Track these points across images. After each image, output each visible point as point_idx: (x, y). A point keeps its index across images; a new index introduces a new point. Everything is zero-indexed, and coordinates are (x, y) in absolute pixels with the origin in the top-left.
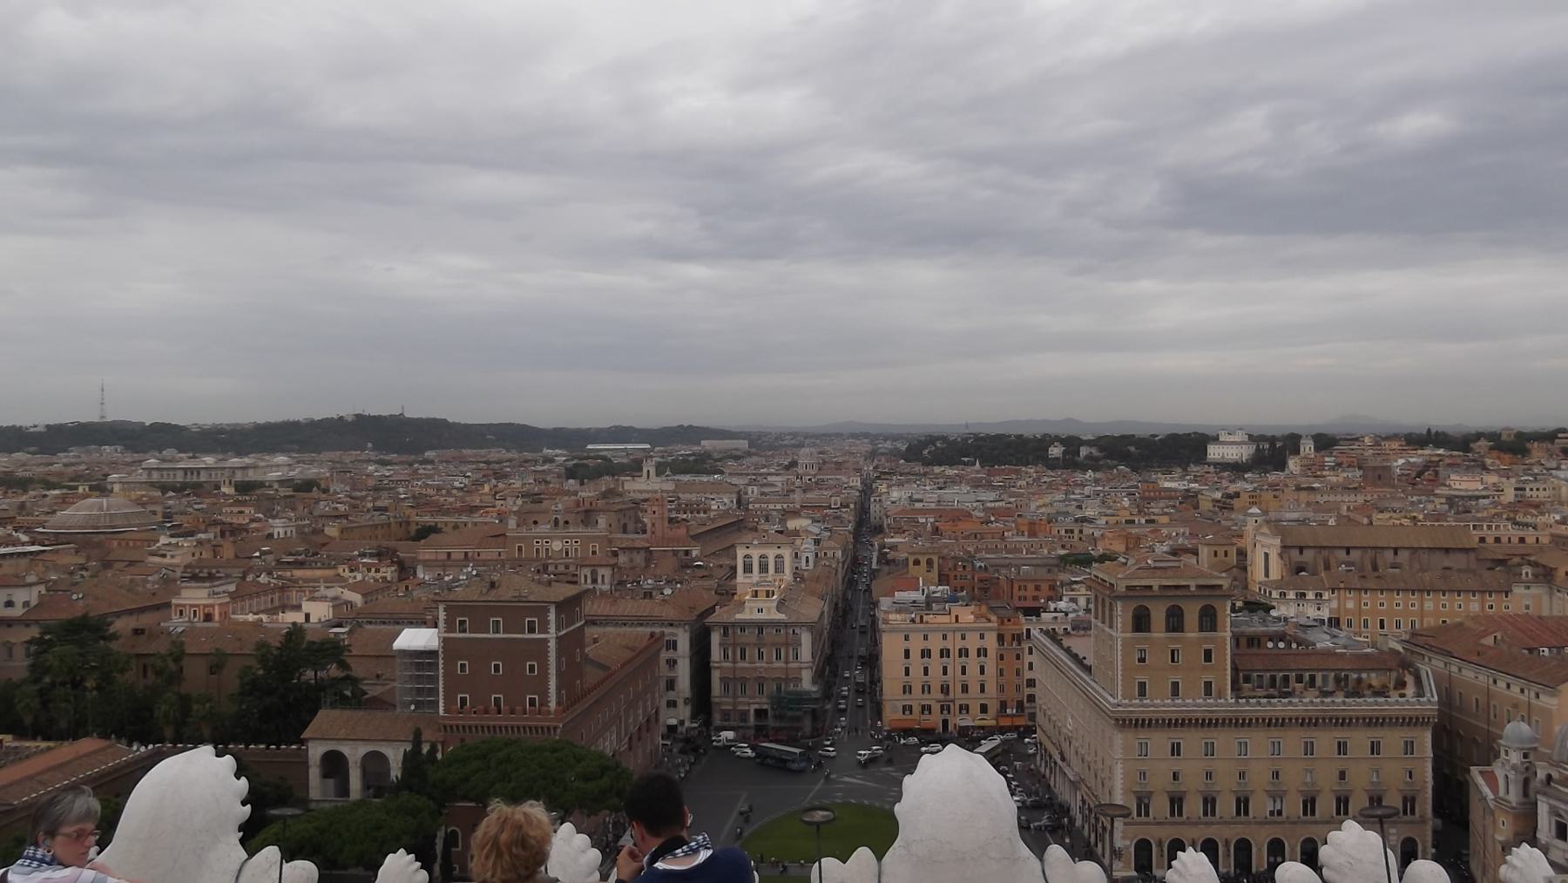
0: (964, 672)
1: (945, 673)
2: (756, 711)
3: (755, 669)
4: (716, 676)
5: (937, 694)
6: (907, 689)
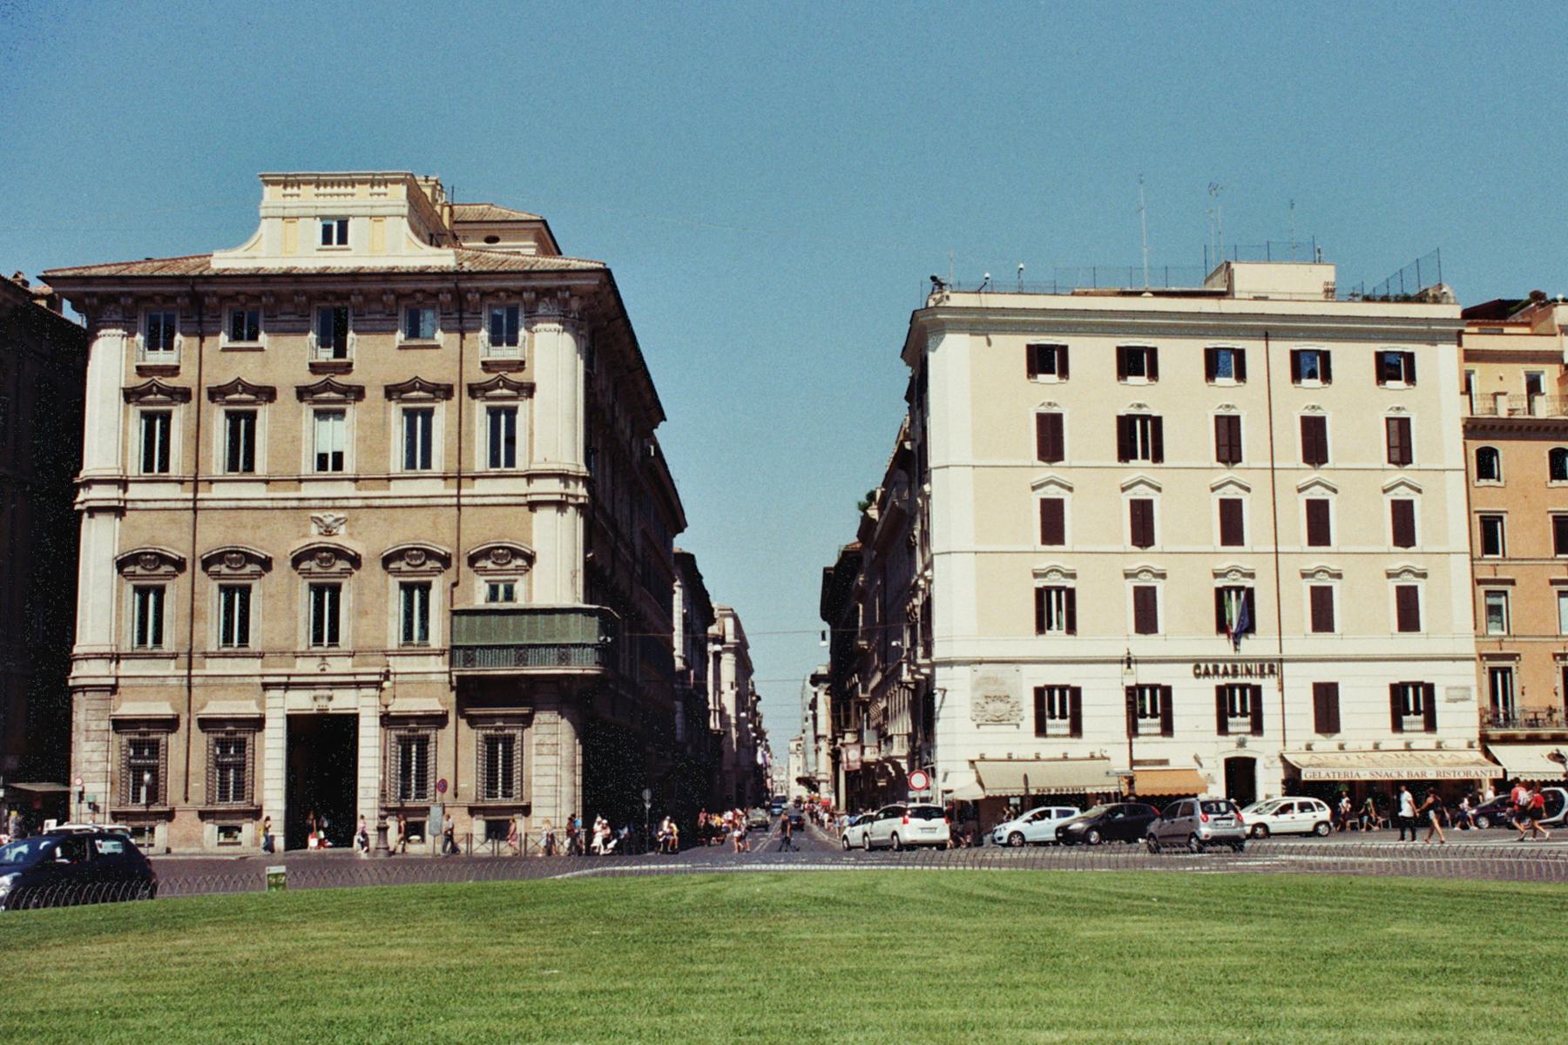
0: (1319, 531)
1: (1232, 531)
2: (297, 725)
3: (301, 507)
4: (99, 544)
5: (1188, 628)
6: (1054, 607)
